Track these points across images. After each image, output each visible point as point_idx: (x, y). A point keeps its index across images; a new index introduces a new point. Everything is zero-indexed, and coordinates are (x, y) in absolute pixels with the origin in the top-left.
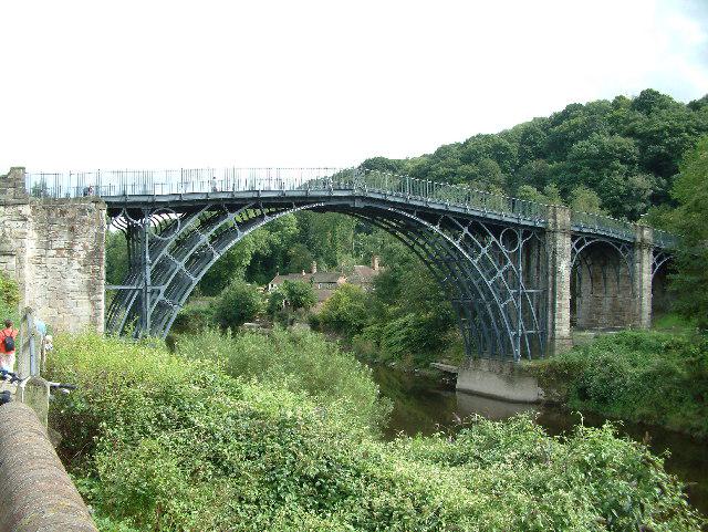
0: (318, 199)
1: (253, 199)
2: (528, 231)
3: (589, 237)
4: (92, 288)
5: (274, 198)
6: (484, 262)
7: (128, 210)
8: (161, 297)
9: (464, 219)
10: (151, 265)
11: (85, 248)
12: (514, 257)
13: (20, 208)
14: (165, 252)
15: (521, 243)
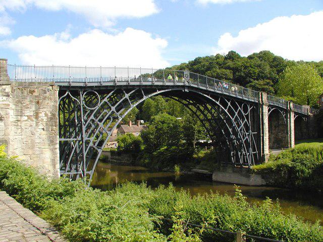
0: (168, 87)
1: (137, 86)
2: (252, 104)
3: (272, 106)
4: (52, 142)
5: (149, 86)
6: (236, 119)
7: (71, 92)
8: (91, 144)
9: (229, 98)
10: (84, 125)
11: (46, 115)
12: (247, 116)
13: (4, 87)
14: (92, 117)
15: (249, 110)
